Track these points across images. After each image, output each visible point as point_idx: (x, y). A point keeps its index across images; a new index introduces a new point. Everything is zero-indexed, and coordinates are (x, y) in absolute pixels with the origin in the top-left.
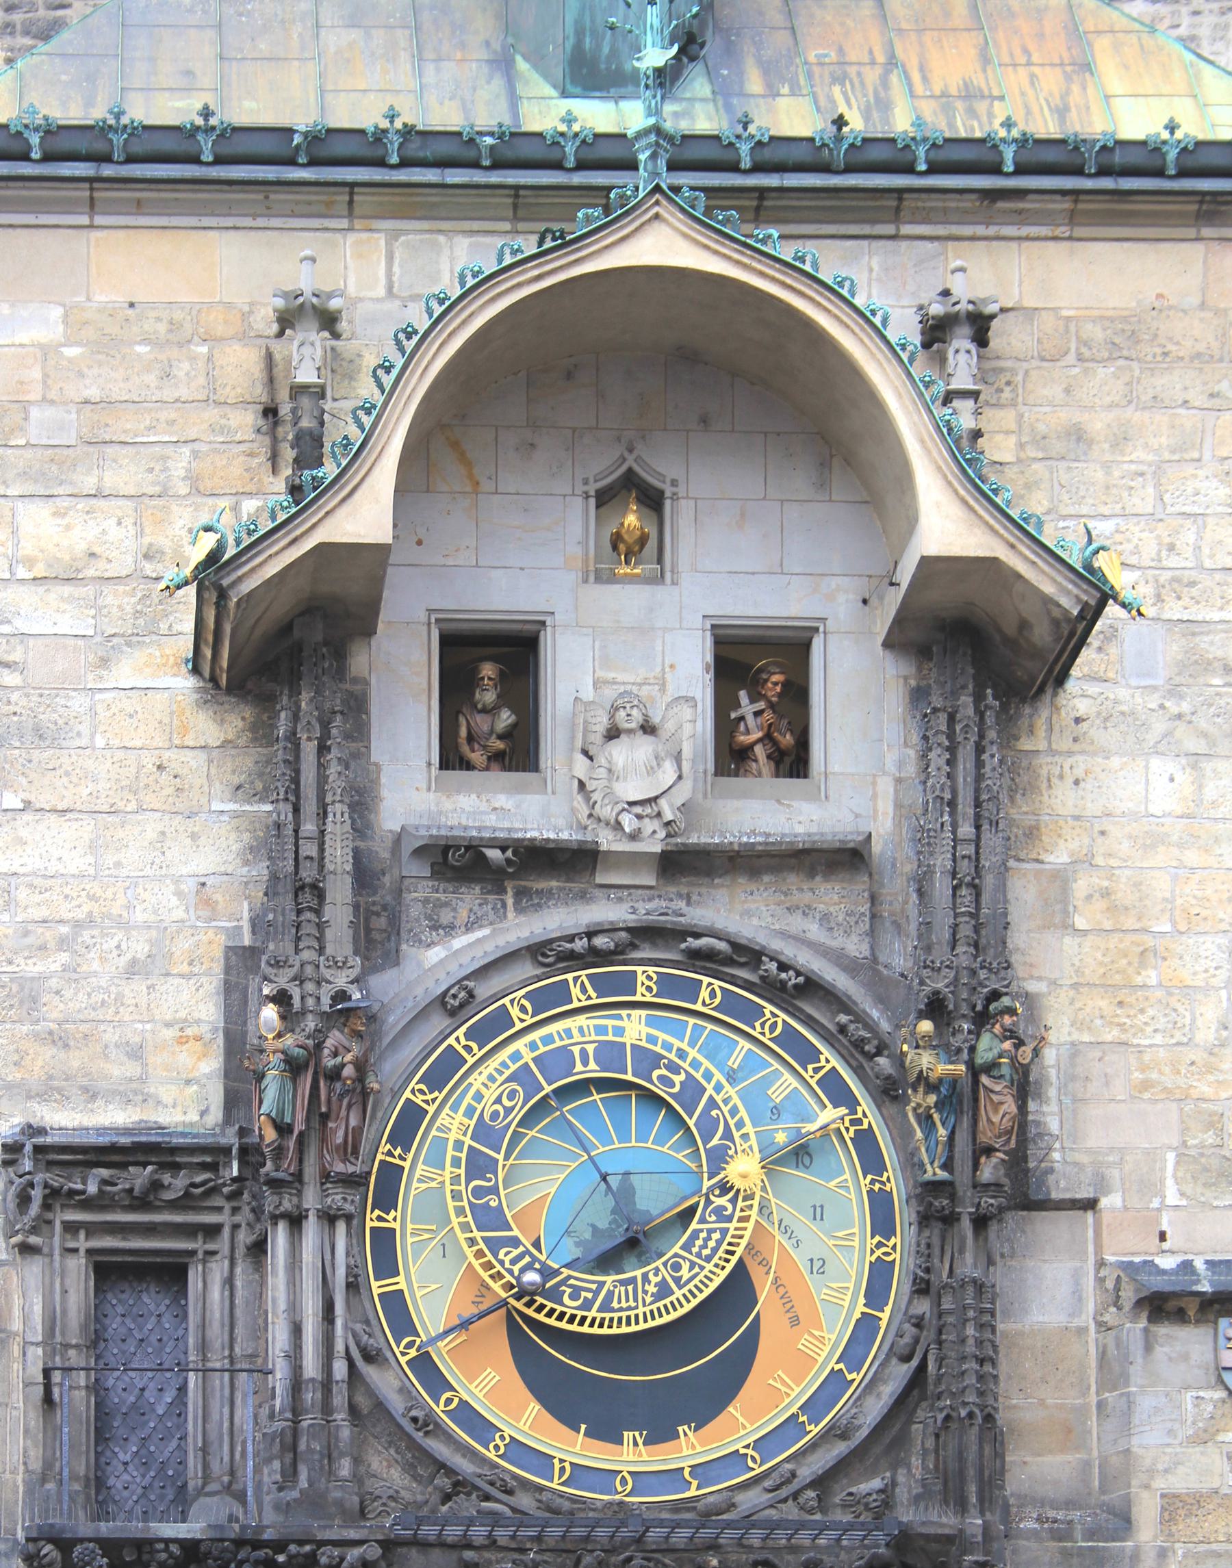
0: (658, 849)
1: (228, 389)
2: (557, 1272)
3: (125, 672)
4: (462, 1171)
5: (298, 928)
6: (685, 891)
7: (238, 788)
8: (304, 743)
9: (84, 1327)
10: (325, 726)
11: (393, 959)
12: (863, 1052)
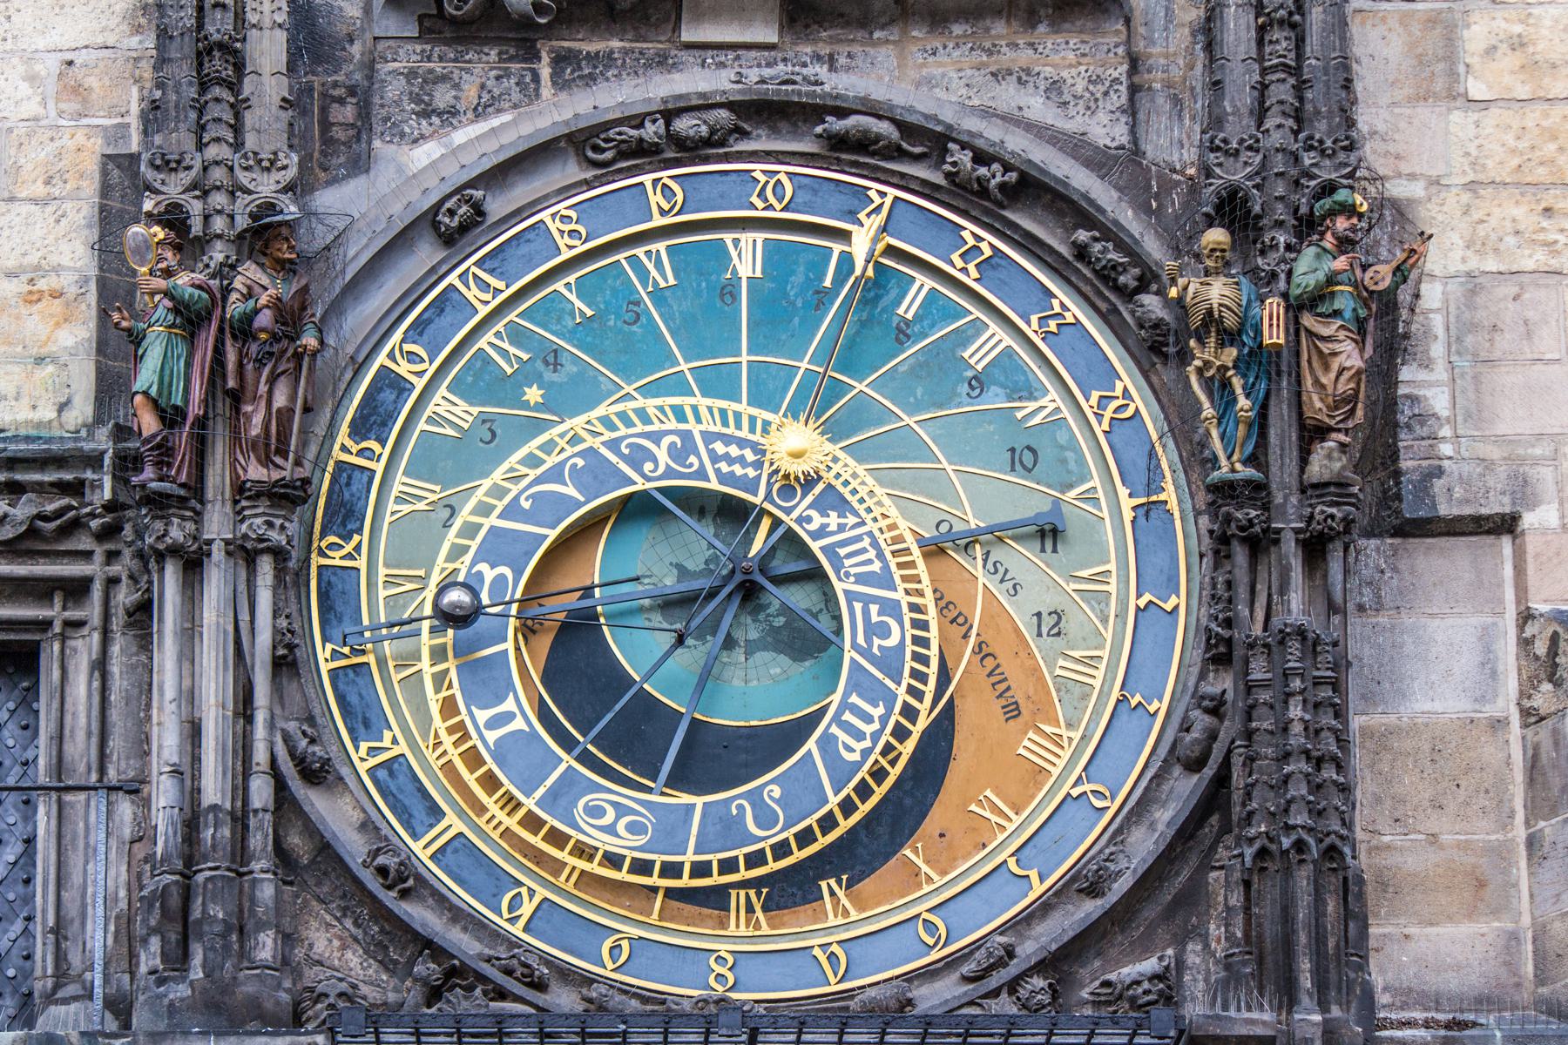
6: (825, 50)
11: (360, 164)
12: (1119, 290)
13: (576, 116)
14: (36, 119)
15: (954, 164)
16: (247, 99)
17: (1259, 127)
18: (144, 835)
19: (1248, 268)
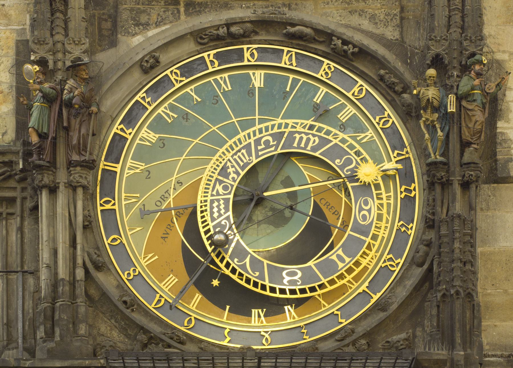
11: (113, 44)
12: (395, 92)
13: (194, 26)
15: (335, 45)
16: (69, 18)
17: (448, 31)
18: (38, 290)
19: (443, 84)
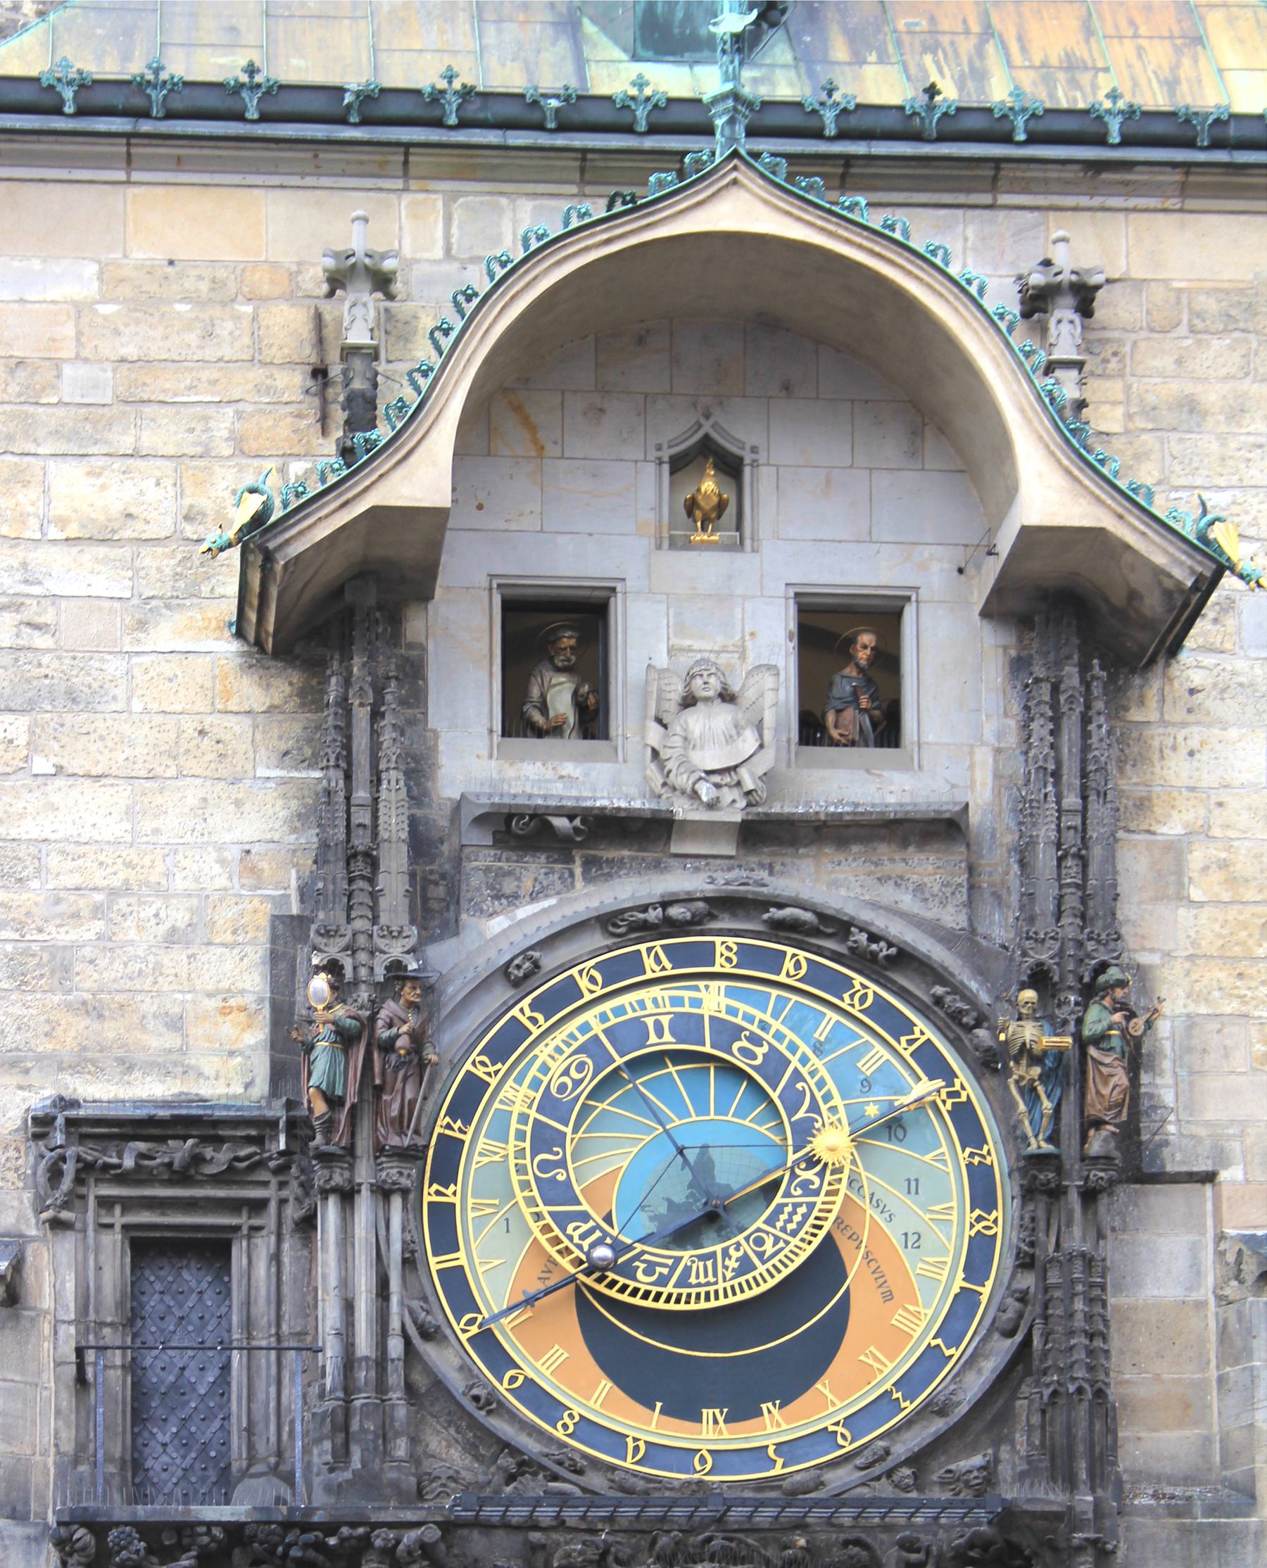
0: (738, 818)
1: (274, 349)
2: (629, 1248)
3: (164, 635)
4: (527, 1145)
5: (350, 897)
6: (767, 860)
7: (286, 754)
8: (356, 709)
9: (120, 1305)
10: (379, 692)
11: (452, 928)
14: (225, 889)
